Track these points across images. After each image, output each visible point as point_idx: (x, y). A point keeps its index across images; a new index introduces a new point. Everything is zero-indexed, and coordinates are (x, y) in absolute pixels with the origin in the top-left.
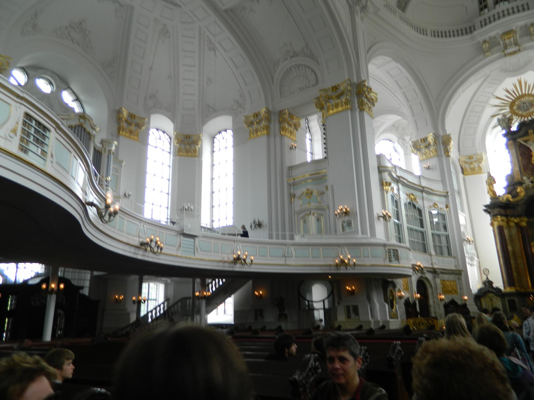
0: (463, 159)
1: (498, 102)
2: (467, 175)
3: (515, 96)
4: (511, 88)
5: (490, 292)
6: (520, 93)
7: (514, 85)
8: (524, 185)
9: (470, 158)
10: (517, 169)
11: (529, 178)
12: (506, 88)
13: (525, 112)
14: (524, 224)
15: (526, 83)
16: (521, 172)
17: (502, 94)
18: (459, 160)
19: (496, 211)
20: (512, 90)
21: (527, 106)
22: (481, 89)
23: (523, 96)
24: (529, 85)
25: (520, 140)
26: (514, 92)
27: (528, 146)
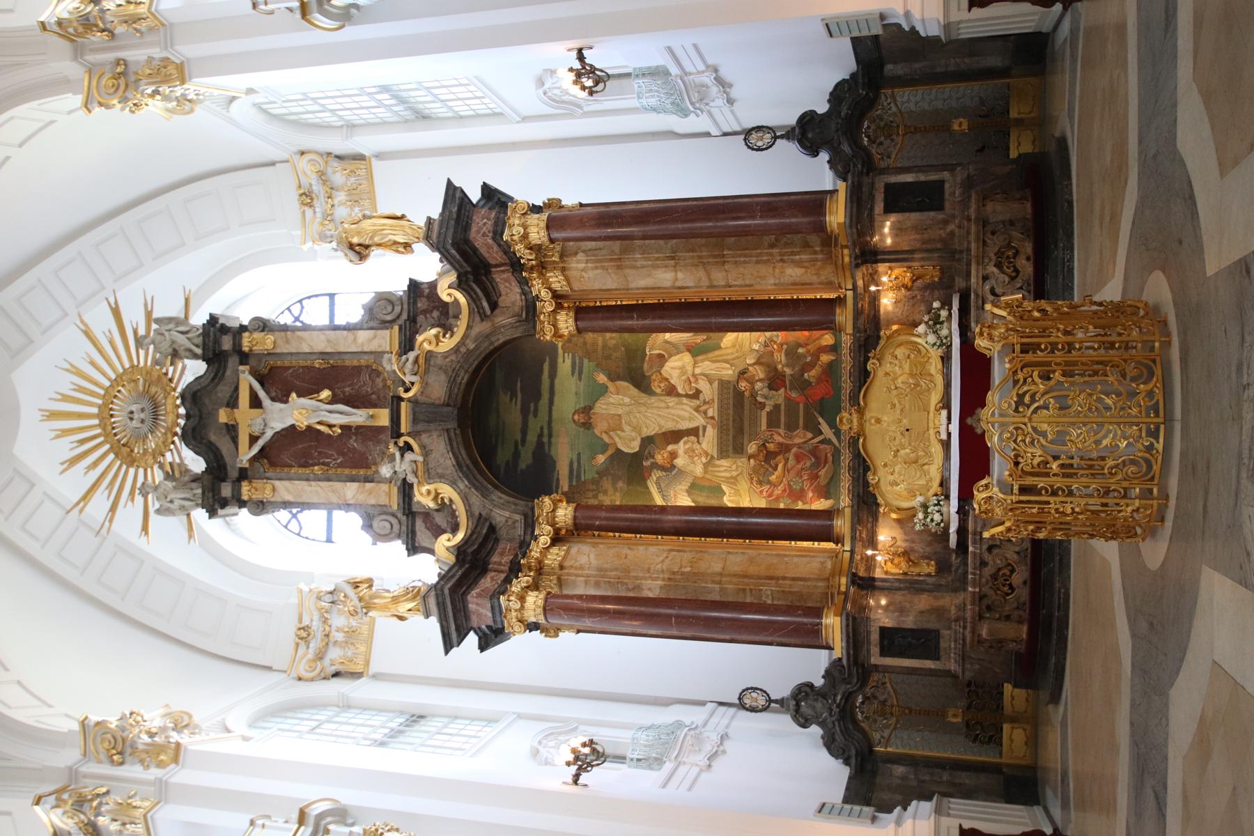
0: (302, 669)
1: (100, 503)
2: (367, 663)
3: (102, 439)
4: (66, 447)
5: (846, 713)
6: (96, 422)
7: (57, 437)
8: (411, 479)
9: (304, 634)
10: (351, 490)
11: (392, 459)
12: (62, 464)
13: (160, 420)
14: (565, 514)
15: (66, 398)
16: (367, 480)
17: (80, 479)
18: (300, 679)
19: (478, 607)
20: (75, 444)
21: (143, 410)
22: (32, 548)
23: (105, 414)
24: (74, 390)
25: (246, 455)
26: (82, 442)
27: (269, 434)
